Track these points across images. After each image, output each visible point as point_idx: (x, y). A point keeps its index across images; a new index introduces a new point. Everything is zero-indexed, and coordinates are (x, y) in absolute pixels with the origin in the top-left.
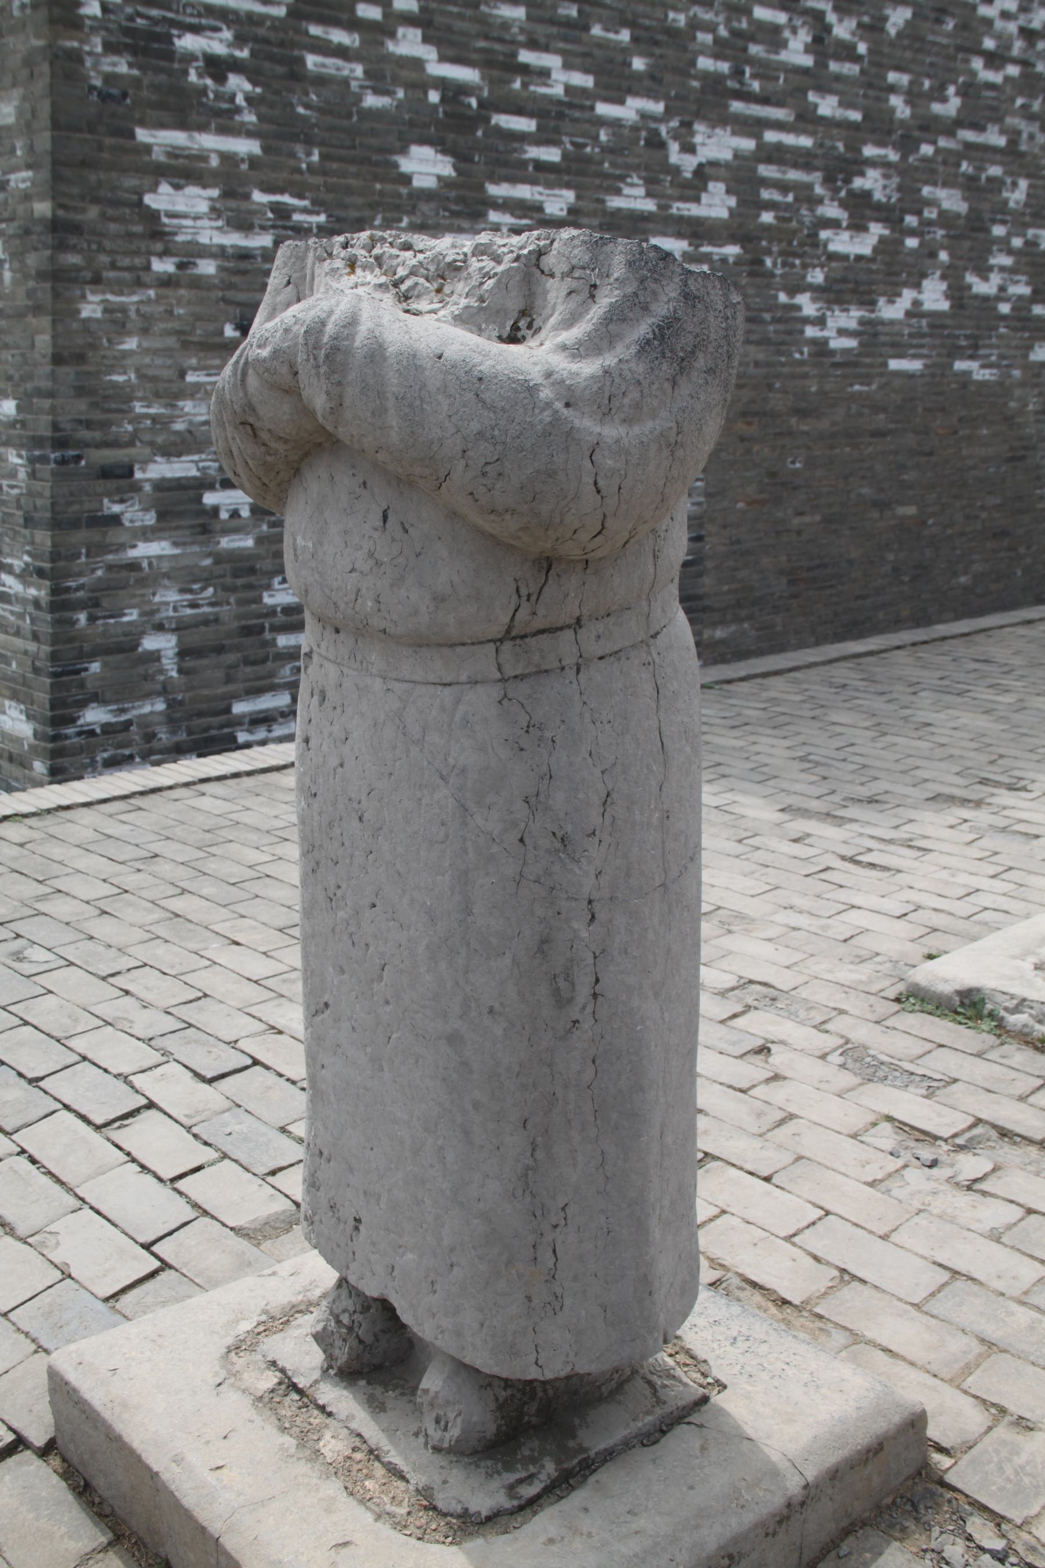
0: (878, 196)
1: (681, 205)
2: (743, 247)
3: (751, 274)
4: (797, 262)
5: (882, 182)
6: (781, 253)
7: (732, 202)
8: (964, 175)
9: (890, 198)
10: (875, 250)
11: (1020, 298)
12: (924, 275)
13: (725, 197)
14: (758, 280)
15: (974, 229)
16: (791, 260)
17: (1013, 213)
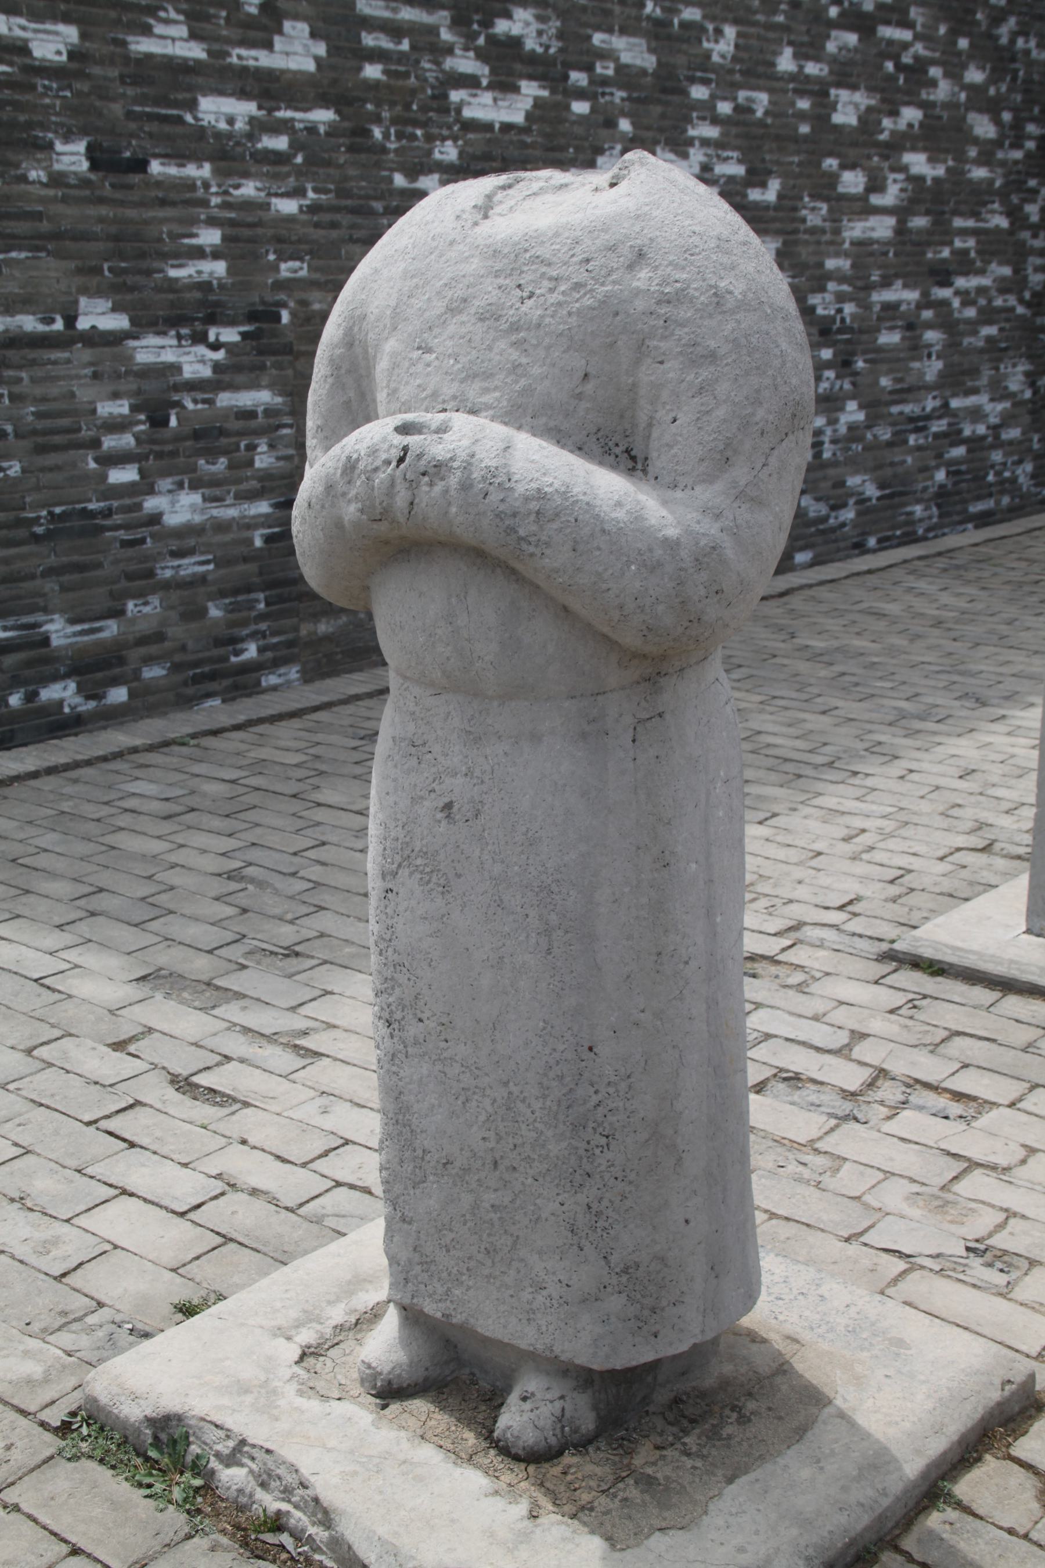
0: (531, 44)
1: (244, 52)
2: (338, 112)
3: (352, 149)
4: (419, 132)
5: (535, 26)
6: (394, 121)
7: (321, 49)
8: (649, 18)
9: (547, 47)
10: (529, 116)
12: (599, 151)
13: (310, 42)
14: (363, 157)
15: (664, 90)
16: (409, 129)
17: (716, 69)
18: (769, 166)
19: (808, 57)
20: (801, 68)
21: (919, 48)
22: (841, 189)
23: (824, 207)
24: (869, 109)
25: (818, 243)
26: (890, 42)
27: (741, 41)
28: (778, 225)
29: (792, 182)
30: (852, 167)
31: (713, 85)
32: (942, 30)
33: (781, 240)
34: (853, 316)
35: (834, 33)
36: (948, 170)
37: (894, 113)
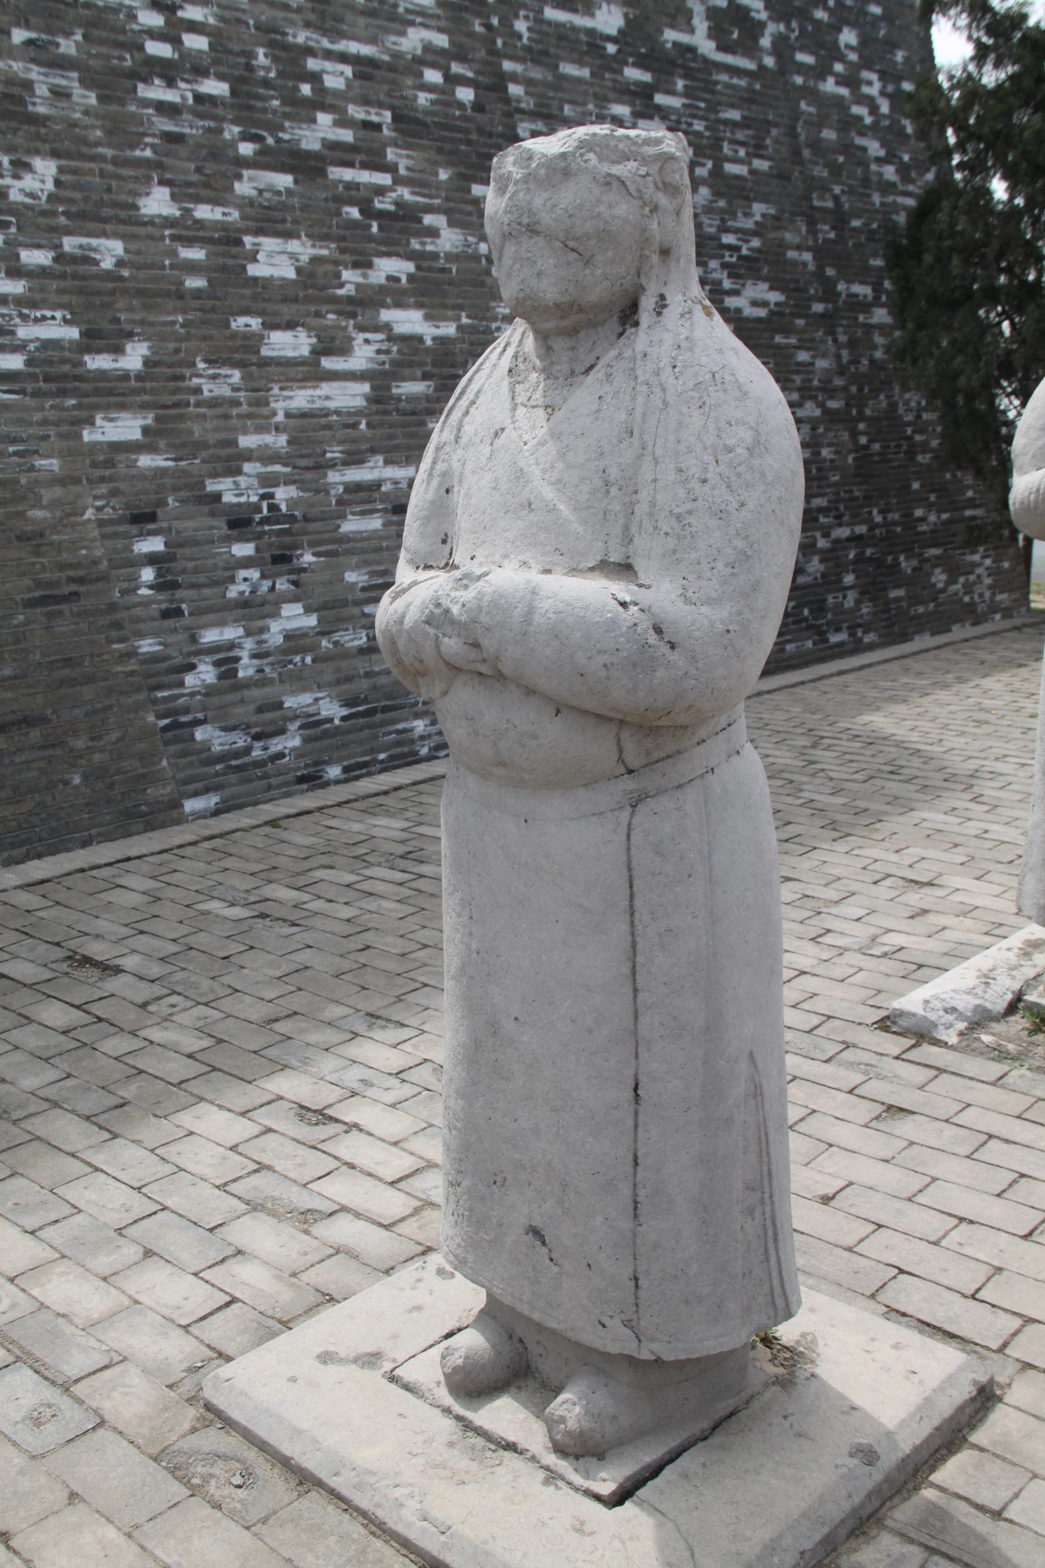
11: (47, 344)
18: (127, 327)
19: (199, 200)
20: (188, 211)
21: (405, 193)
22: (265, 352)
23: (236, 376)
24: (315, 260)
25: (226, 417)
26: (351, 186)
27: (65, 178)
28: (146, 398)
29: (171, 346)
30: (290, 326)
31: (13, 230)
32: (443, 175)
33: (152, 415)
34: (291, 503)
35: (246, 173)
36: (460, 328)
37: (364, 264)
